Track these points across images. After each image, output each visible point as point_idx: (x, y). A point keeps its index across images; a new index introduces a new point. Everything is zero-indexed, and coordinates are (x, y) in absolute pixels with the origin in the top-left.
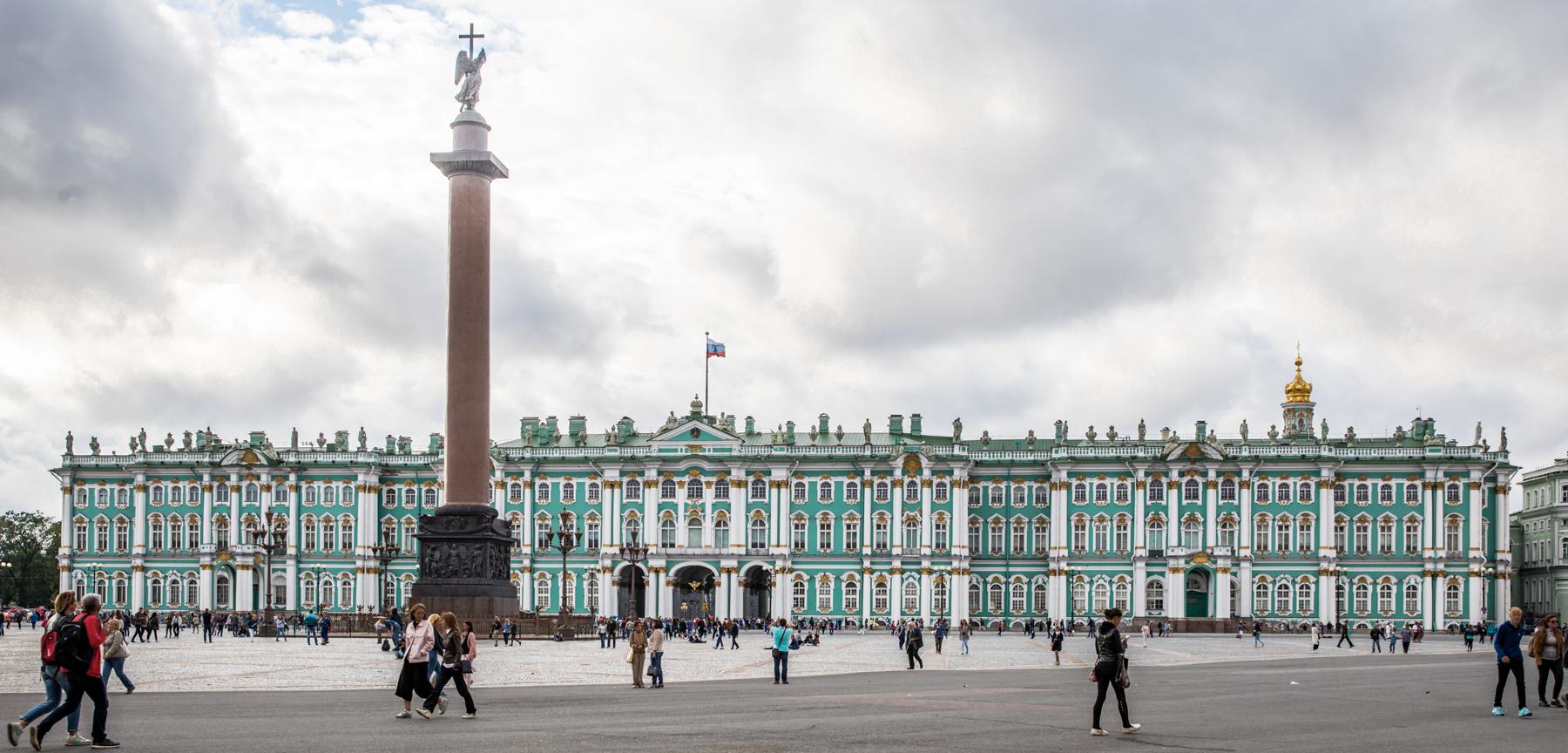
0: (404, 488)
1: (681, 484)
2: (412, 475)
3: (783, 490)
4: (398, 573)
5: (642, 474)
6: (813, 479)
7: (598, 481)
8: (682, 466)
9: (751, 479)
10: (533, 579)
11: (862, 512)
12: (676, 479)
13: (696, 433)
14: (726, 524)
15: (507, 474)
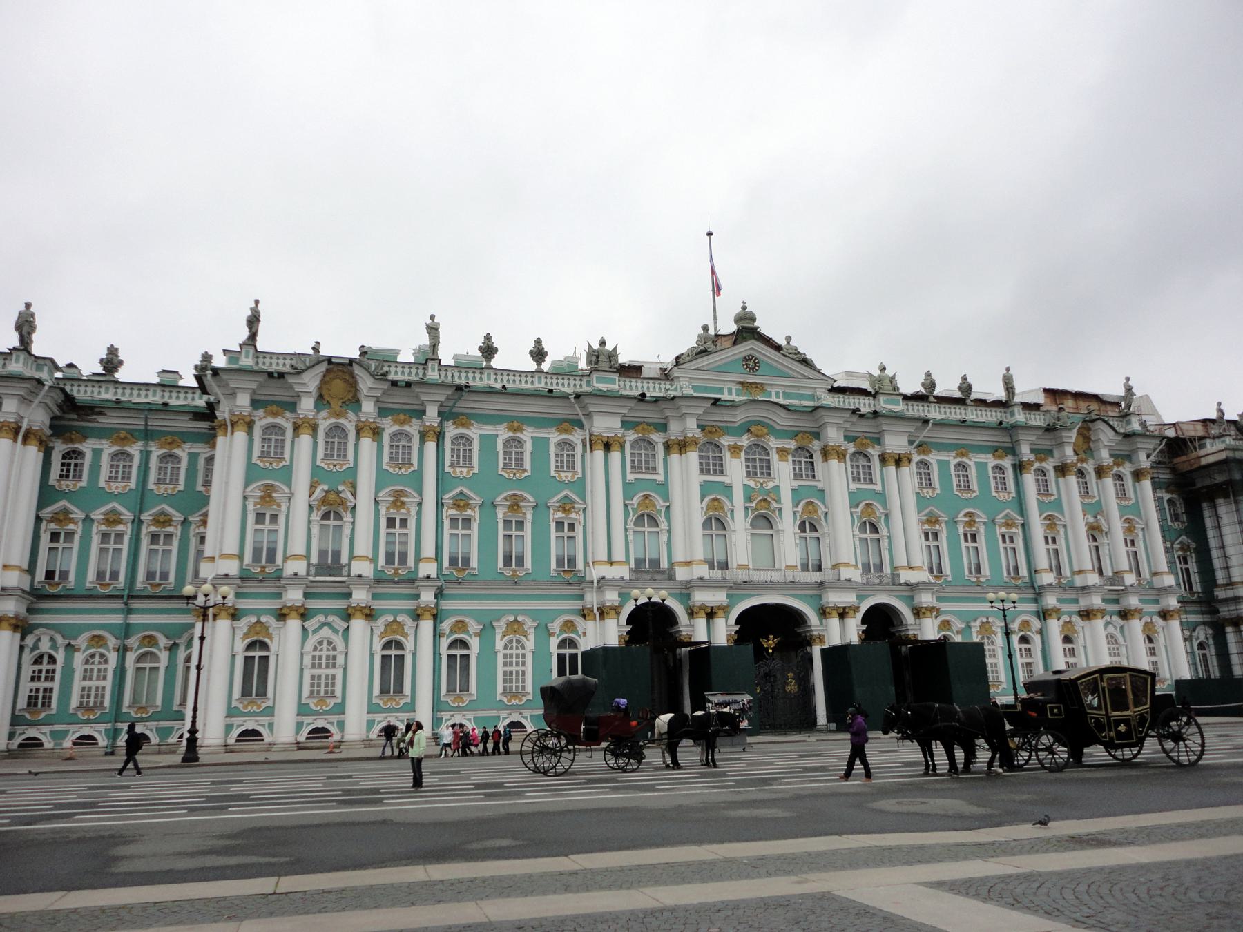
0: (108, 449)
1: (735, 450)
2: (137, 422)
3: (905, 470)
4: (69, 632)
5: (663, 427)
6: (943, 456)
7: (576, 437)
8: (739, 417)
9: (851, 448)
10: (437, 635)
11: (1022, 511)
12: (725, 441)
13: (751, 363)
14: (814, 528)
15: (382, 412)
